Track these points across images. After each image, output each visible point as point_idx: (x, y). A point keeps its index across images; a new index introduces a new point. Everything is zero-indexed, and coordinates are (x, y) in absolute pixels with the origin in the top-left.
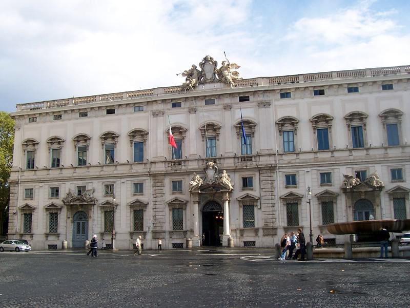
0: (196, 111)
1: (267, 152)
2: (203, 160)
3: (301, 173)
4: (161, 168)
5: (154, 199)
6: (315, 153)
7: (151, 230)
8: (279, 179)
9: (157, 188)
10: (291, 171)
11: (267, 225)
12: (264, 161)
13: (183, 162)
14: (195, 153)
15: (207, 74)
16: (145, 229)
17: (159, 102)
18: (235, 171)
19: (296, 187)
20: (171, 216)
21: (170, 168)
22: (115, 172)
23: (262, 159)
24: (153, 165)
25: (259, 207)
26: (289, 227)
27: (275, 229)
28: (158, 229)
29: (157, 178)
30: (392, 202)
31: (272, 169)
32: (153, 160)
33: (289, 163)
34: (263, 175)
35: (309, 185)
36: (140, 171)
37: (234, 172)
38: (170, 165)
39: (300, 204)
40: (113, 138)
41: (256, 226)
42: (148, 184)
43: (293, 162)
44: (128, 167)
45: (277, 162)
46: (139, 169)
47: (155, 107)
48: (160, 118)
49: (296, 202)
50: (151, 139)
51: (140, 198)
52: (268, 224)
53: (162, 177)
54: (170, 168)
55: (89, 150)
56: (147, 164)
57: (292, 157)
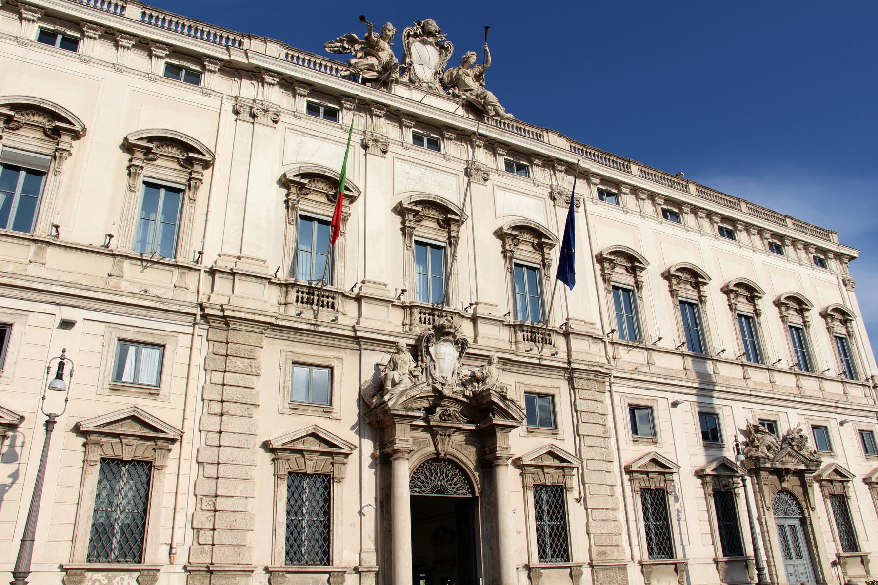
0: (385, 152)
2: (408, 308)
4: (264, 301)
5: (213, 423)
7: (181, 559)
9: (230, 378)
10: (642, 396)
11: (604, 553)
14: (382, 280)
15: (416, 66)
16: (155, 551)
17: (269, 79)
20: (282, 506)
21: (293, 310)
22: (34, 270)
24: (222, 284)
25: (577, 497)
27: (623, 567)
28: (222, 558)
29: (233, 336)
30: (829, 502)
32: (226, 264)
34: (584, 394)
35: (680, 443)
36: (154, 292)
38: (293, 295)
40: (54, 134)
42: (188, 351)
44: (107, 264)
46: (159, 282)
47: (248, 89)
48: (262, 130)
50: (216, 184)
51: (149, 408)
52: (608, 550)
53: (253, 338)
54: (293, 310)
56: (192, 277)
57: (638, 357)
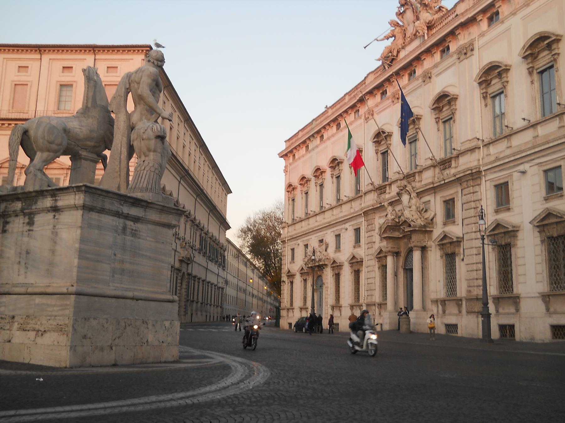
1: (468, 146)
3: (516, 175)
6: (534, 126)
8: (486, 194)
12: (466, 163)
13: (388, 188)
18: (434, 189)
19: (509, 209)
23: (462, 160)
26: (555, 292)
31: (474, 176)
33: (497, 159)
37: (435, 193)
39: (515, 245)
41: (459, 295)
43: (502, 155)
45: (481, 163)
49: (509, 240)
55: (325, 187)
